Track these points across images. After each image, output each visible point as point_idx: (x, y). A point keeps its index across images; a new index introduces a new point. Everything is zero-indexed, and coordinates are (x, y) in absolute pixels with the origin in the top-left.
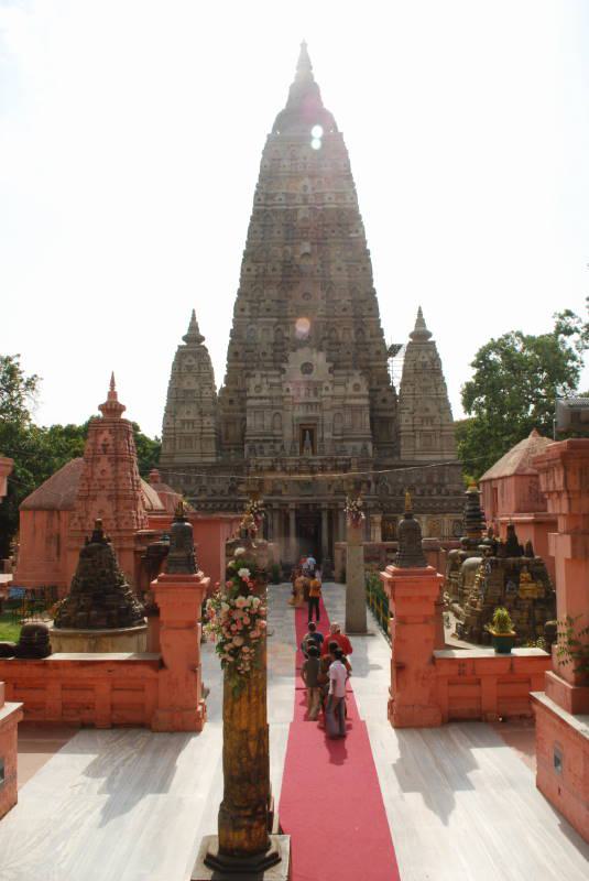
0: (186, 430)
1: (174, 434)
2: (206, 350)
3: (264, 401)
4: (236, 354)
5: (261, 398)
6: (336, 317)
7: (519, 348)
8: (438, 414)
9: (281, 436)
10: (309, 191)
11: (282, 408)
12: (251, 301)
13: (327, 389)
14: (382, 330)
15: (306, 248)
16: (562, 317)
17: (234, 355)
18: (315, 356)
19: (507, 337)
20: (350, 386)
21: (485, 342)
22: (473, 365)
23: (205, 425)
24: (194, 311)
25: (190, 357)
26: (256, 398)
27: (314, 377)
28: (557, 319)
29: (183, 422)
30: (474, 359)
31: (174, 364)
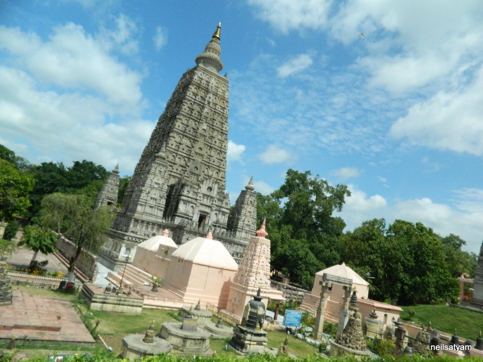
0: (150, 203)
1: (146, 203)
5: (188, 197)
6: (209, 163)
8: (252, 225)
9: (192, 217)
10: (211, 101)
11: (195, 204)
12: (176, 142)
13: (215, 201)
14: (225, 175)
20: (224, 203)
23: (161, 203)
25: (161, 167)
26: (185, 196)
29: (151, 198)
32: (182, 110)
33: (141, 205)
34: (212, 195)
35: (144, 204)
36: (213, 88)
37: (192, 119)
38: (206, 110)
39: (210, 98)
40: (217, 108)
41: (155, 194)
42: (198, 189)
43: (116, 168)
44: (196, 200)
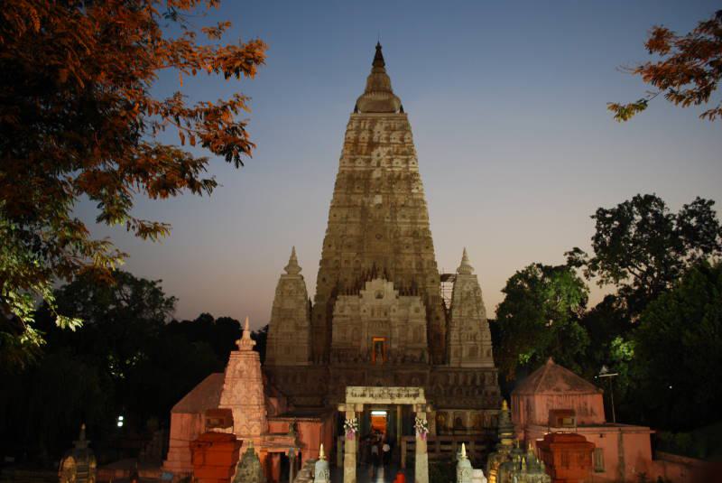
2: (303, 278)
3: (345, 319)
4: (324, 280)
7: (540, 275)
15: (379, 199)
16: (571, 253)
17: (322, 279)
18: (385, 285)
19: (530, 268)
20: (412, 308)
21: (513, 273)
22: (503, 291)
24: (294, 248)
27: (384, 302)
28: (568, 256)
30: (505, 285)
31: (277, 289)
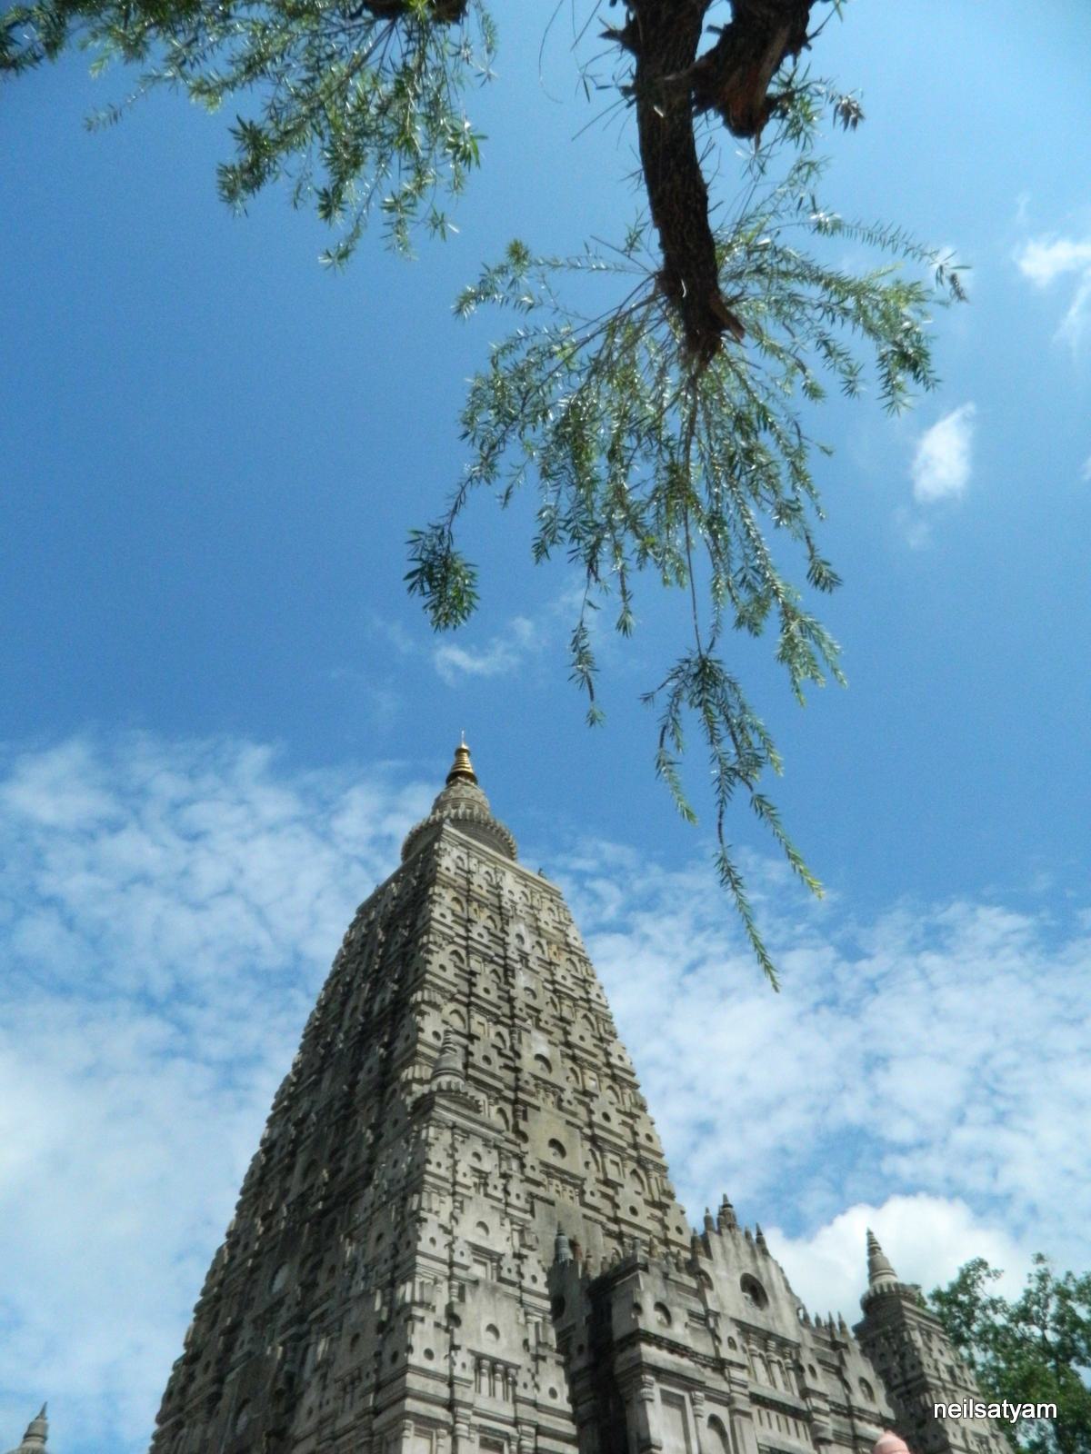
1: (450, 1405)
3: (685, 1362)
5: (674, 1347)
11: (727, 1401)
32: (429, 967)
33: (427, 1425)
34: (779, 1329)
35: (441, 1413)
36: (519, 907)
37: (482, 1010)
38: (522, 980)
39: (519, 937)
40: (558, 978)
41: (493, 1329)
42: (699, 1294)
43: (27, 1436)
44: (720, 1365)
